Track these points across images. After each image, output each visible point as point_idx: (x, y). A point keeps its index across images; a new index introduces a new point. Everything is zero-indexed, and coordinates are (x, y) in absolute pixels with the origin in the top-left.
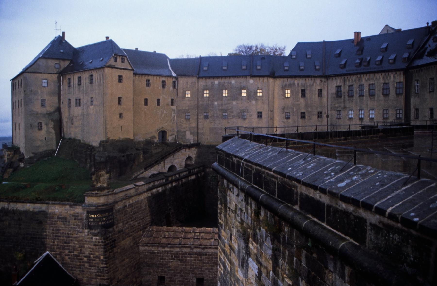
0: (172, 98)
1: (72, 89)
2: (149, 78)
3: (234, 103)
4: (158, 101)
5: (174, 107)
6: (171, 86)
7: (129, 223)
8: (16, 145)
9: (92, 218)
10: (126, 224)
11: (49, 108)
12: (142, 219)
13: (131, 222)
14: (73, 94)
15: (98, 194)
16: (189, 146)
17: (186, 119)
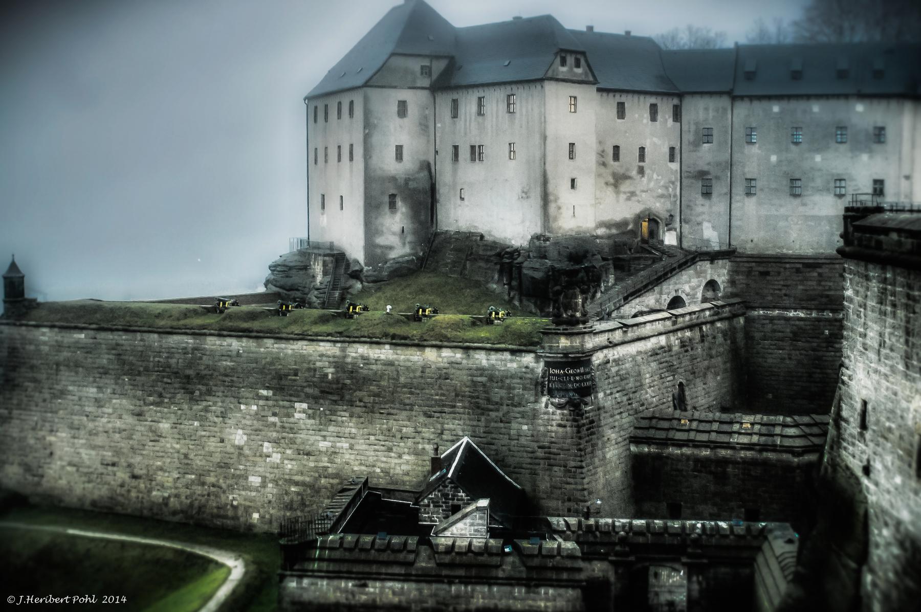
0: (673, 144)
1: (462, 123)
2: (623, 98)
3: (818, 158)
4: (642, 150)
5: (675, 166)
6: (669, 117)
7: (613, 396)
8: (632, 216)
9: (554, 375)
10: (609, 395)
11: (408, 165)
12: (634, 392)
13: (617, 395)
14: (466, 134)
15: (567, 329)
16: (713, 257)
17: (836, 195)
